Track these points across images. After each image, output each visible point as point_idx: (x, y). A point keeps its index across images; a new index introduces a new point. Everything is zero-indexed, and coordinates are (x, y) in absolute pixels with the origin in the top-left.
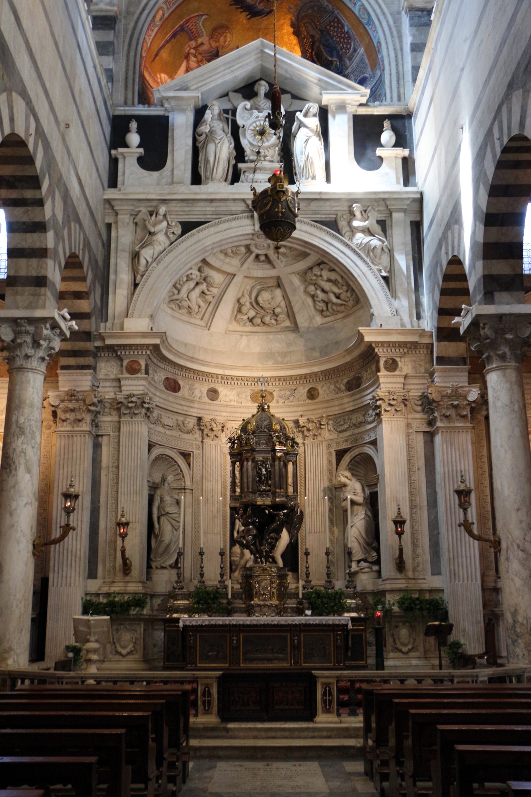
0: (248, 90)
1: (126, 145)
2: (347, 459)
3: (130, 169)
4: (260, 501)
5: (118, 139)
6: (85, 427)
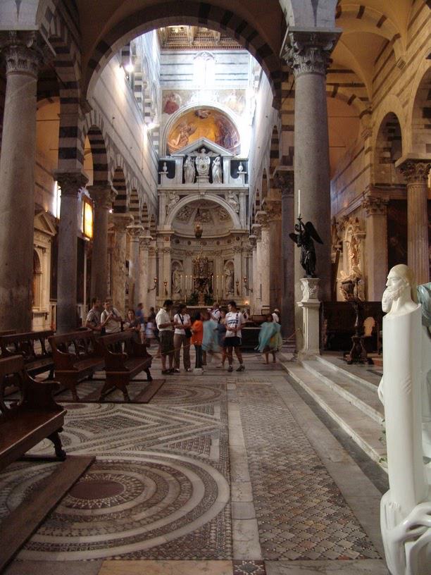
0: (199, 150)
1: (163, 171)
2: (227, 263)
3: (164, 178)
4: (201, 277)
5: (160, 169)
6: (155, 257)
